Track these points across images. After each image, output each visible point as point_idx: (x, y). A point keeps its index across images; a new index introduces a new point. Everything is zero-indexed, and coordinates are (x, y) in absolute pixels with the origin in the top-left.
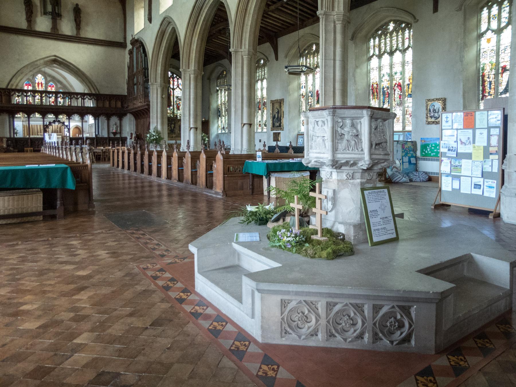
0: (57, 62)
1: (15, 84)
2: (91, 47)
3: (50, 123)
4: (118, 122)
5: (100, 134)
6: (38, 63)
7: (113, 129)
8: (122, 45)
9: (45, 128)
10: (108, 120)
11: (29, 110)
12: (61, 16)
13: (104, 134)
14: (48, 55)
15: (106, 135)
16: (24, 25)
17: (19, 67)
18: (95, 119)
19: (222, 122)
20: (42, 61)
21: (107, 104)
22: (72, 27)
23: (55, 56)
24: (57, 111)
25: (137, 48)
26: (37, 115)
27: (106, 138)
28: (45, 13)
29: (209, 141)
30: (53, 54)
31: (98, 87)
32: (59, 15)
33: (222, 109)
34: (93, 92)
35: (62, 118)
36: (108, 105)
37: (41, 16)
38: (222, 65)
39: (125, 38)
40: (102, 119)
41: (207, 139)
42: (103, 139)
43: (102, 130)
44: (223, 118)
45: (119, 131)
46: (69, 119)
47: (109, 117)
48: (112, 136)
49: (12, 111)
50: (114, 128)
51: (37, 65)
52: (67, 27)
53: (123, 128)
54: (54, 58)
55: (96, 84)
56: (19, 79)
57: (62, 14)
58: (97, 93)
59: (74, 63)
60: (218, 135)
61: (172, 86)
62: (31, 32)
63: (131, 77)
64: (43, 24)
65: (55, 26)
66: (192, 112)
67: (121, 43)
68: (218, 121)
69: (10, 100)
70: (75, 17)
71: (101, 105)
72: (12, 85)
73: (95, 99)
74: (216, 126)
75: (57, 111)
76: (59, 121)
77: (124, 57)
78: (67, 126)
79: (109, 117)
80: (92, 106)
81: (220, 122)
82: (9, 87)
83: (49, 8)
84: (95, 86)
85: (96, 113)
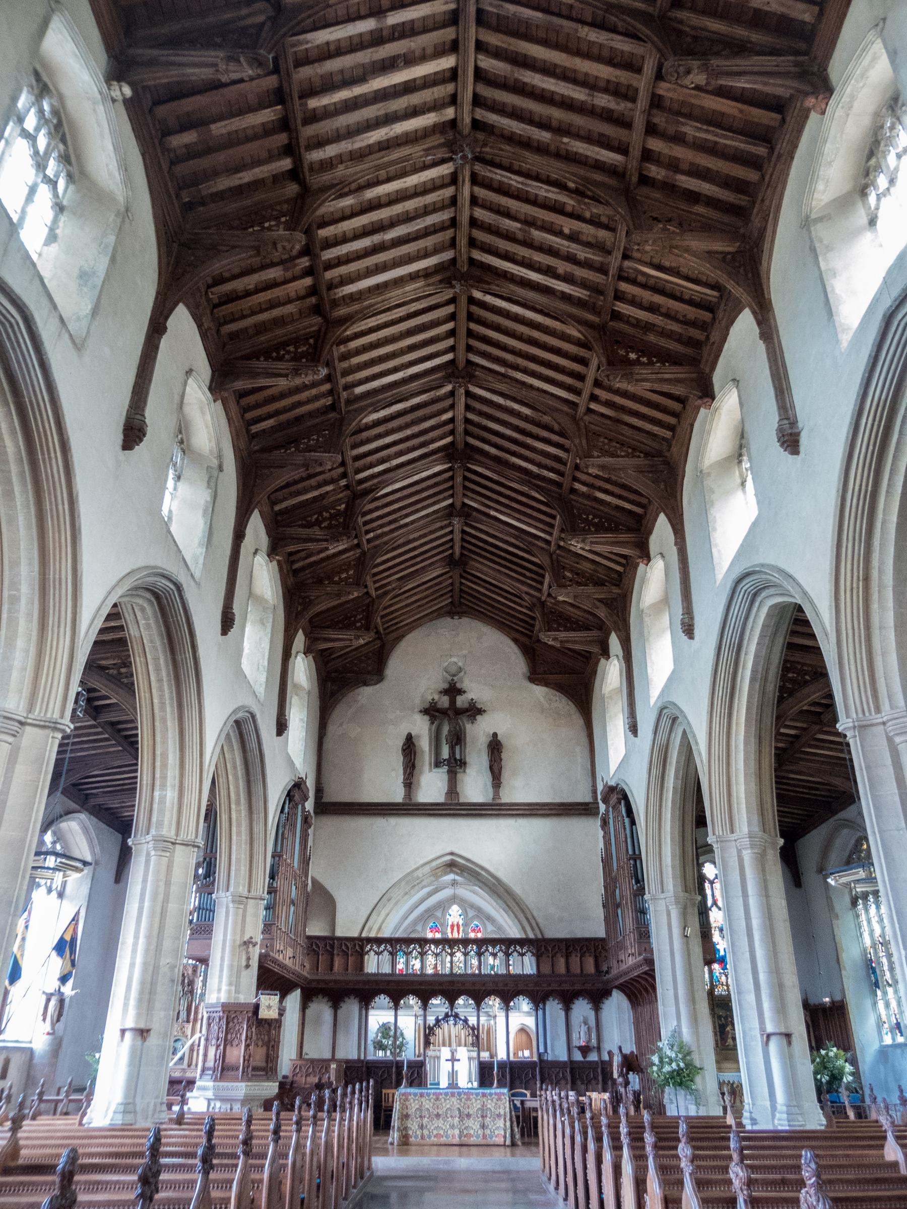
1: (376, 927)
2: (522, 822)
3: (438, 1021)
6: (419, 873)
7: (579, 1039)
8: (585, 810)
9: (428, 1035)
10: (567, 1009)
11: (397, 989)
12: (465, 763)
13: (559, 1052)
14: (438, 854)
15: (564, 1057)
16: (397, 795)
17: (383, 887)
19: (887, 1005)
20: (427, 869)
21: (561, 968)
22: (486, 785)
23: (452, 854)
24: (450, 988)
26: (412, 1000)
27: (565, 1062)
28: (438, 764)
29: (856, 1074)
30: (448, 850)
31: (540, 921)
32: (462, 764)
33: (880, 963)
37: (430, 770)
39: (594, 792)
40: (554, 1007)
41: (848, 1068)
42: (556, 1064)
43: (552, 1040)
44: (890, 990)
45: (594, 1042)
47: (567, 1000)
48: (578, 1056)
49: (367, 991)
51: (418, 878)
52: (475, 786)
53: (605, 1034)
54: (449, 858)
55: (535, 914)
56: (383, 914)
57: (468, 760)
58: (540, 936)
60: (884, 1053)
64: (432, 786)
65: (453, 790)
67: (587, 804)
68: (875, 1004)
70: (491, 761)
71: (546, 969)
72: (370, 930)
73: (533, 954)
74: (872, 1020)
75: (450, 988)
76: (456, 1016)
78: (473, 1028)
79: (567, 1000)
81: (881, 1005)
82: (364, 935)
83: (445, 753)
85: (538, 991)
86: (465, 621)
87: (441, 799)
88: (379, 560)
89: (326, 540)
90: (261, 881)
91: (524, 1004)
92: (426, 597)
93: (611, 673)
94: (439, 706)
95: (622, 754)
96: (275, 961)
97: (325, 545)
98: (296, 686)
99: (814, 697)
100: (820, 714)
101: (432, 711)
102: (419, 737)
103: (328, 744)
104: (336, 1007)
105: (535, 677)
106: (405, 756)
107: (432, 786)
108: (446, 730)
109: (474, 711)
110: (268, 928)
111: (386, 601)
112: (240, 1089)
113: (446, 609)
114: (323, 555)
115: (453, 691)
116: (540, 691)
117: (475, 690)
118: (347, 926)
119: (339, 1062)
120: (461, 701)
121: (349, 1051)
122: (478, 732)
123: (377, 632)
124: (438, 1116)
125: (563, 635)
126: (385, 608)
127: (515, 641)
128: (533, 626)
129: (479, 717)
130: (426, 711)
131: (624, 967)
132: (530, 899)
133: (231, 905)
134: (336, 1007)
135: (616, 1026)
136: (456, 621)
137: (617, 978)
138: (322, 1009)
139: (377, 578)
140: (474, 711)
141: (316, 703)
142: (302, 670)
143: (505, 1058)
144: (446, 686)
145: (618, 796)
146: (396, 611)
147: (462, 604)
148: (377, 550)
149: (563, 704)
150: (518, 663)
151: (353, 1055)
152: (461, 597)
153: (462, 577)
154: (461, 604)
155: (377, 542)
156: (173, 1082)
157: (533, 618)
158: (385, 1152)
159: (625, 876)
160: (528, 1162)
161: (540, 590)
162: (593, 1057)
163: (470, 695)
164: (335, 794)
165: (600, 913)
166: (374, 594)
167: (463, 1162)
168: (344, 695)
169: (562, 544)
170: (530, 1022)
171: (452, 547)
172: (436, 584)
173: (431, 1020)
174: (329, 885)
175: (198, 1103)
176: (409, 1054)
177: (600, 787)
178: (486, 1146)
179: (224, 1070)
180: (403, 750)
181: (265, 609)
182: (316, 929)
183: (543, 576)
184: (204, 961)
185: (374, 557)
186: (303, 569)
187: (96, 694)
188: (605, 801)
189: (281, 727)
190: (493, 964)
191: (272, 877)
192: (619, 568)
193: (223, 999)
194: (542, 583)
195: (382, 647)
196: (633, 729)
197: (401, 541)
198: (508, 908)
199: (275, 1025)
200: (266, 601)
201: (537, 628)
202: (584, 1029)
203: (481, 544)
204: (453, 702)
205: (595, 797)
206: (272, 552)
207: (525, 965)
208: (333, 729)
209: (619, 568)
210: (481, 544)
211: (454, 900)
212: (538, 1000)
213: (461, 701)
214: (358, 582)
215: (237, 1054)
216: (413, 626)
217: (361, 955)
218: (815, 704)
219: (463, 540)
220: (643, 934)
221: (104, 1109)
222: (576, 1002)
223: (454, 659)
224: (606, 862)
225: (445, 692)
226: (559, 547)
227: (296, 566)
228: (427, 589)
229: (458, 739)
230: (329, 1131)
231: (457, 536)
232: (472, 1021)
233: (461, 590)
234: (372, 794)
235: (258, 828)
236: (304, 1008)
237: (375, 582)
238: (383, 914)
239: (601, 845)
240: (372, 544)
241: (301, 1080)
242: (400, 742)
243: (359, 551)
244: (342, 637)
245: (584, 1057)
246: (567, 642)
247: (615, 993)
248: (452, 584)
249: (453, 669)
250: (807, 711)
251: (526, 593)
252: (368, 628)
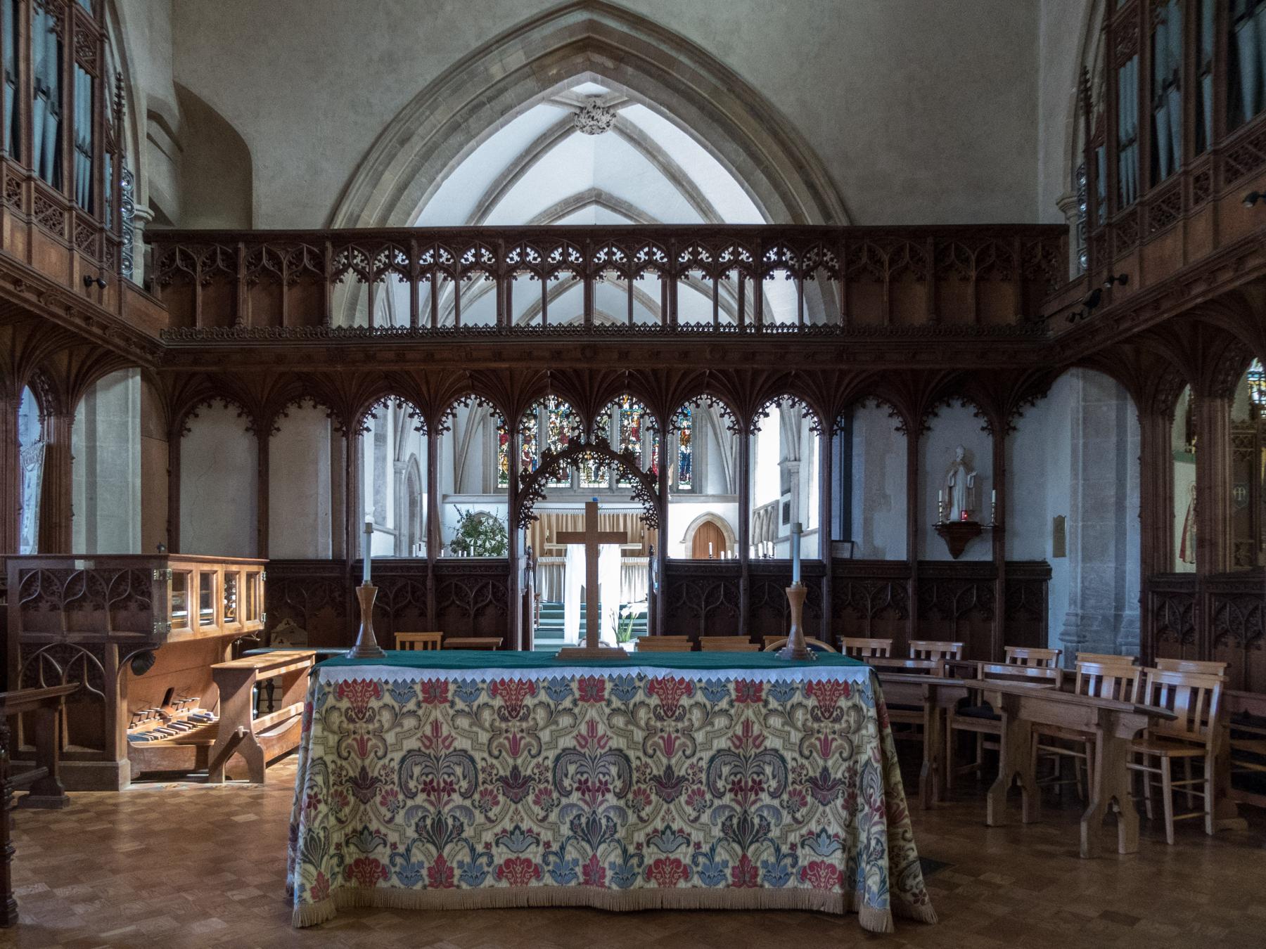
4: (984, 446)
5: (857, 537)
10: (916, 432)
18: (827, 433)
35: (625, 419)
40: (879, 429)
43: (869, 509)
48: (939, 551)
50: (958, 494)
69: (318, 310)
75: (589, 368)
76: (603, 448)
84: (832, 182)
104: (261, 432)
134: (261, 432)
162: (980, 552)
202: (961, 482)
222: (944, 411)
245: (956, 552)
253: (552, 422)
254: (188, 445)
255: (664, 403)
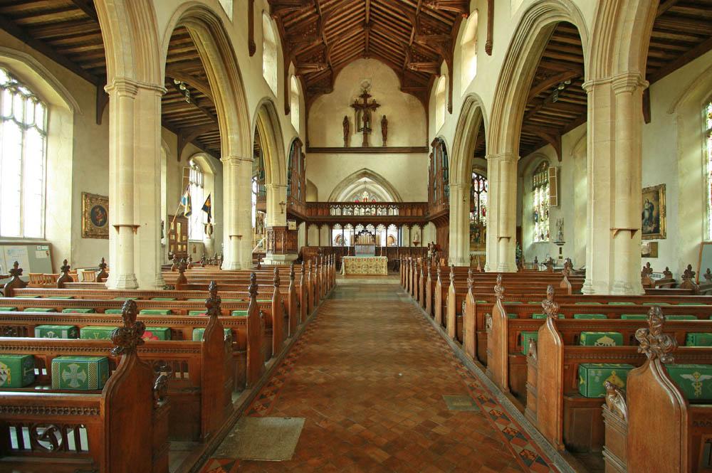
0: (366, 173)
3: (359, 232)
6: (352, 177)
8: (423, 150)
9: (356, 237)
10: (410, 229)
11: (343, 221)
13: (406, 244)
16: (342, 144)
17: (337, 182)
24: (365, 221)
25: (437, 148)
26: (349, 226)
28: (359, 130)
32: (370, 130)
34: (397, 201)
35: (370, 228)
36: (410, 214)
38: (542, 155)
39: (428, 142)
42: (405, 248)
45: (420, 241)
46: (375, 228)
47: (410, 226)
48: (413, 245)
49: (331, 223)
52: (376, 140)
56: (337, 193)
59: (381, 174)
61: (476, 189)
62: (347, 150)
63: (432, 180)
64: (357, 140)
65: (366, 141)
66: (502, 215)
71: (403, 214)
75: (365, 221)
76: (367, 231)
77: (424, 161)
78: (373, 236)
79: (410, 226)
80: (395, 214)
83: (362, 125)
85: (399, 222)
86: (371, 60)
87: (360, 145)
88: (328, 23)
89: (300, 6)
90: (285, 180)
91: (392, 227)
92: (352, 46)
93: (441, 84)
94: (359, 103)
95: (444, 123)
96: (293, 211)
97: (298, 8)
98: (294, 93)
99: (543, 90)
100: (544, 99)
101: (356, 106)
102: (350, 118)
103: (309, 122)
104: (319, 228)
105: (403, 89)
106: (344, 127)
107: (357, 140)
108: (362, 114)
109: (375, 106)
110: (289, 198)
111: (332, 49)
112: (283, 257)
113: (363, 53)
114: (299, 18)
115: (365, 96)
116: (405, 96)
117: (376, 96)
118: (323, 198)
119: (322, 247)
120: (369, 101)
121: (326, 244)
122: (377, 115)
123: (329, 66)
124: (359, 267)
125: (418, 64)
126: (332, 52)
127: (395, 70)
128: (404, 61)
129: (377, 108)
130: (353, 106)
131: (435, 213)
132: (397, 188)
133: (273, 189)
134: (319, 228)
135: (429, 235)
136: (366, 60)
137: (432, 217)
138: (313, 229)
139: (327, 34)
140: (375, 106)
141: (304, 103)
142: (294, 84)
143: (385, 246)
144: (363, 93)
145: (440, 143)
146: (338, 54)
147: (369, 51)
148: (327, 16)
149: (416, 102)
150: (396, 82)
151: (327, 245)
152: (369, 46)
153: (370, 34)
154: (370, 51)
155: (328, 10)
156: (255, 255)
157: (404, 57)
158: (341, 278)
159: (439, 178)
160: (396, 281)
161: (408, 40)
162: (419, 246)
163: (373, 98)
164: (313, 145)
165: (426, 192)
166: (327, 44)
167: (370, 281)
168: (316, 99)
169: (422, 9)
170: (395, 234)
171: (365, 16)
172: (357, 39)
173: (357, 233)
174: (313, 182)
175: (268, 261)
176: (348, 244)
177: (431, 141)
178: (378, 276)
179: (276, 251)
180: (344, 124)
181: (272, 48)
182: (310, 199)
183: (411, 31)
184: (265, 211)
185: (325, 20)
186: (290, 26)
187: (195, 92)
188: (433, 145)
189: (287, 111)
190: (381, 212)
191: (289, 178)
192: (451, 24)
193: (274, 225)
194: (410, 36)
195: (332, 73)
196: (450, 110)
197: (338, 11)
198: (388, 191)
199: (295, 233)
200: (272, 43)
201: (406, 60)
202: (416, 236)
203: (379, 13)
204: (365, 101)
205: (428, 144)
206: (272, 13)
207: (395, 212)
208: (311, 114)
209: (451, 24)
210: (379, 13)
211: (365, 189)
212: (399, 226)
213: (369, 101)
214: (318, 34)
215: (281, 245)
216: (346, 63)
217: (329, 209)
218: (542, 94)
219: (371, 11)
220: (446, 199)
221: (228, 264)
223: (366, 80)
224: (431, 171)
225: (362, 96)
226: (421, 12)
227: (286, 25)
228: (353, 41)
229: (367, 119)
230: (318, 273)
231: (368, 8)
232: (373, 233)
233: (369, 43)
234: (330, 145)
235: (281, 157)
236: (307, 228)
237: (327, 36)
238: (337, 193)
239: (429, 164)
240: (324, 12)
241: (307, 253)
242: (342, 120)
243: (317, 16)
244: (313, 68)
246: (421, 68)
247: (429, 223)
248: (364, 39)
249: (366, 85)
250: (539, 98)
251: (402, 42)
252: (324, 62)
253: (360, 228)
254: (309, 230)
255: (376, 225)
